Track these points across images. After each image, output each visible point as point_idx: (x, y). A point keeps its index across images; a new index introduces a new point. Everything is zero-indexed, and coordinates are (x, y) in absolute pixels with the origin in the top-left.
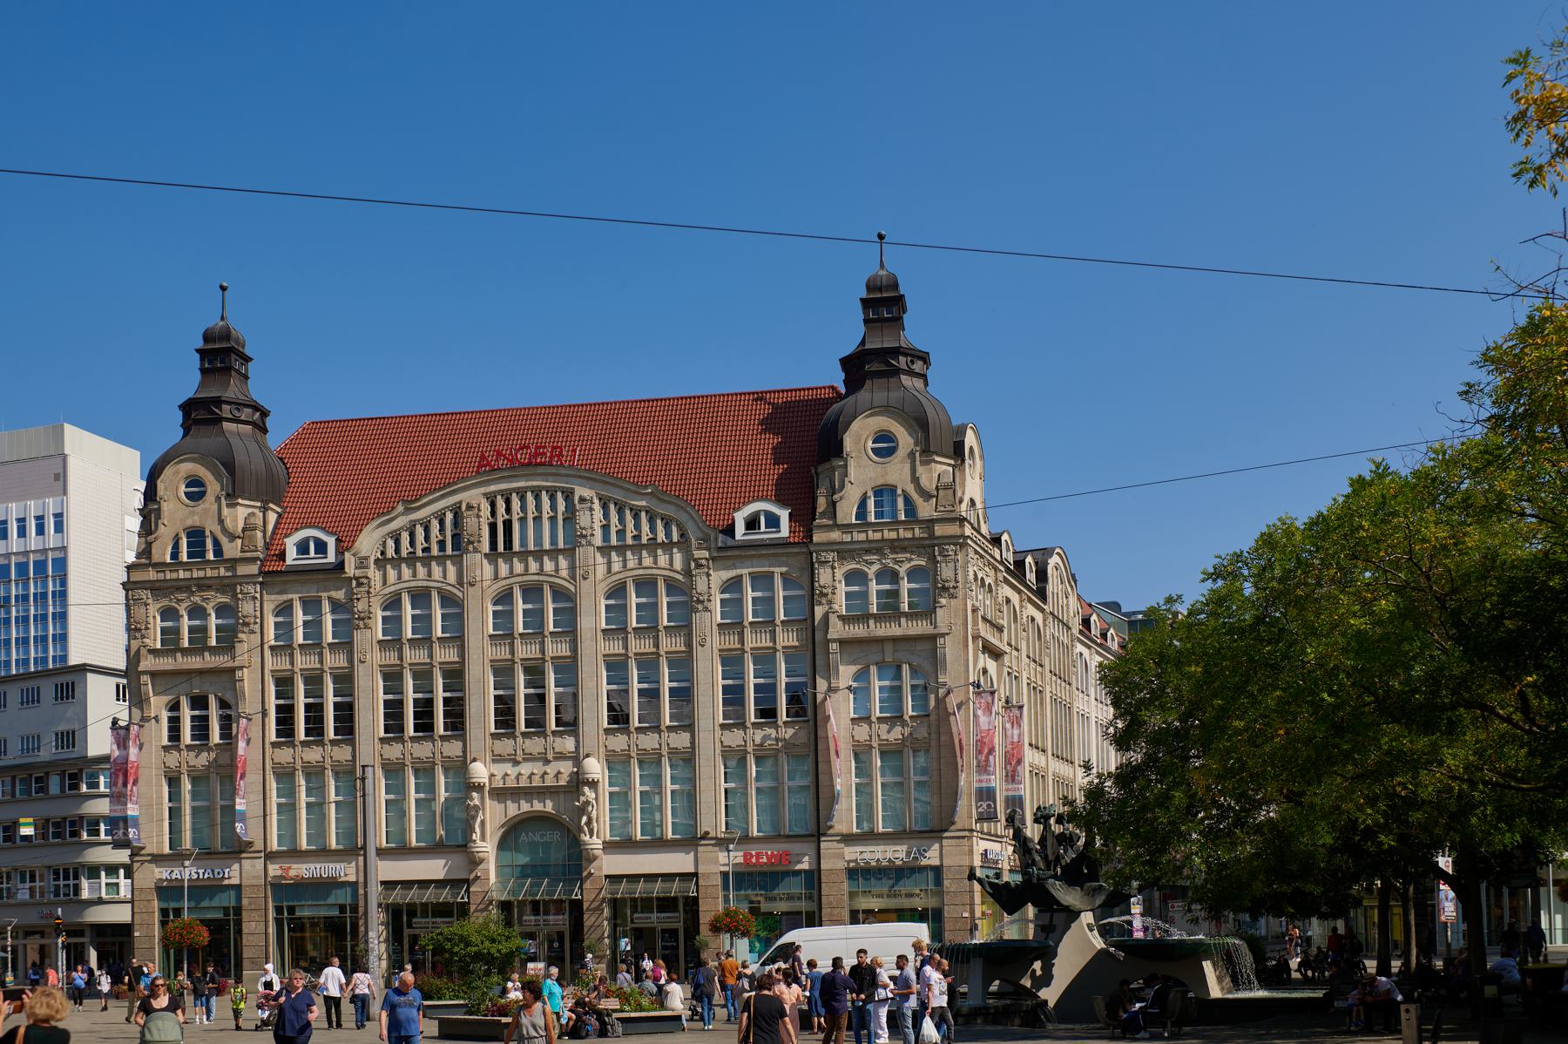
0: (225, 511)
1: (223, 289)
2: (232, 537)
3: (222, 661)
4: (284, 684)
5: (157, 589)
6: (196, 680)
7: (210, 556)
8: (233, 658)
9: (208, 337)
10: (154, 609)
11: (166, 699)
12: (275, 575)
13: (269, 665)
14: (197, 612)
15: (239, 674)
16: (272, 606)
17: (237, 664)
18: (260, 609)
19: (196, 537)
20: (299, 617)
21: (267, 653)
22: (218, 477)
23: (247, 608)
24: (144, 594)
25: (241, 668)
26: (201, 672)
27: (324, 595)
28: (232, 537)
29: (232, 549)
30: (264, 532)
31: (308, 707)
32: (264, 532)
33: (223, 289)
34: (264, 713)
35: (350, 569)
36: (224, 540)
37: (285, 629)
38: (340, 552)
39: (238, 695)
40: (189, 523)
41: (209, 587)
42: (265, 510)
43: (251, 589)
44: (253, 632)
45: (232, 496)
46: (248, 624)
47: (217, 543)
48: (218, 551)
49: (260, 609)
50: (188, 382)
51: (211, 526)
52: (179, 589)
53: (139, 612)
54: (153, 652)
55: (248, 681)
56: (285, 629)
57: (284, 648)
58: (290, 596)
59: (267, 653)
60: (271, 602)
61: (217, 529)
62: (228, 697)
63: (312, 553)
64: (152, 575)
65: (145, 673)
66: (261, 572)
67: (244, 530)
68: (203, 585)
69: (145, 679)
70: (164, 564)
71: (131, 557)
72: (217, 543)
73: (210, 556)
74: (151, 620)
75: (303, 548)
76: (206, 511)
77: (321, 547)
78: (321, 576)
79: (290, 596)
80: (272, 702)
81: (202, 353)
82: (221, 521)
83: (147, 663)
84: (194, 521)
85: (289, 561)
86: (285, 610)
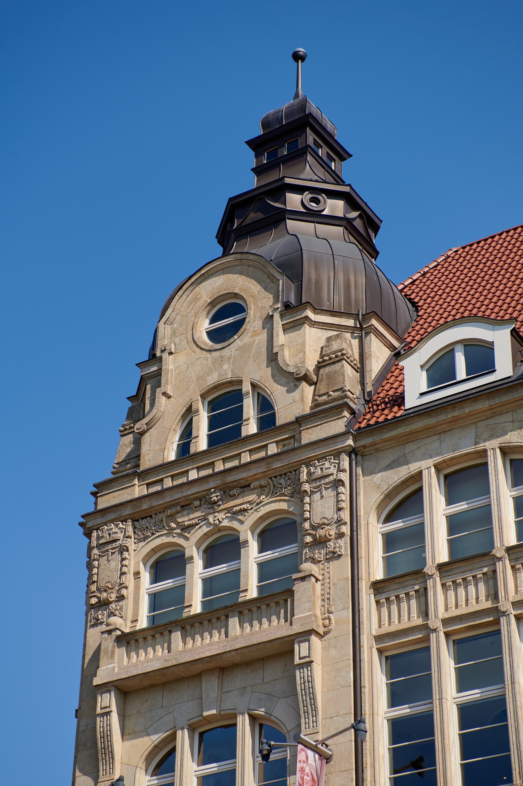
0: (281, 338)
2: (295, 379)
3: (269, 629)
4: (409, 671)
5: (142, 516)
6: (210, 686)
7: (251, 428)
8: (289, 618)
10: (137, 555)
11: (146, 743)
12: (381, 426)
13: (372, 622)
14: (223, 548)
15: (301, 650)
16: (377, 497)
17: (296, 629)
18: (353, 505)
19: (225, 403)
20: (438, 509)
21: (367, 599)
22: (268, 283)
23: (321, 507)
24: (121, 531)
25: (305, 635)
26: (222, 667)
27: (492, 445)
28: (295, 379)
29: (291, 404)
31: (467, 714)
32: (361, 370)
33: (297, 57)
34: (358, 727)
36: (278, 394)
37: (406, 543)
39: (296, 698)
40: (212, 379)
41: (245, 487)
42: (362, 331)
43: (329, 467)
44: (335, 556)
45: (293, 311)
46: (320, 542)
47: (265, 405)
48: (267, 420)
49: (353, 505)
51: (255, 371)
52: (186, 506)
53: (107, 569)
54: (128, 640)
55: (324, 667)
56: (406, 543)
57: (405, 577)
58: (414, 467)
59: (367, 599)
60: (373, 488)
61: (262, 374)
62: (280, 713)
63: (461, 373)
65: (104, 688)
67: (319, 367)
68: (233, 487)
69: (108, 701)
72: (265, 405)
73: (251, 428)
74: (129, 580)
75: (440, 370)
76: (245, 349)
77: (481, 357)
78: (483, 405)
79: (414, 467)
80: (381, 712)
82: (273, 358)
83: (118, 665)
84: (227, 372)
85: (412, 401)
86: (407, 501)
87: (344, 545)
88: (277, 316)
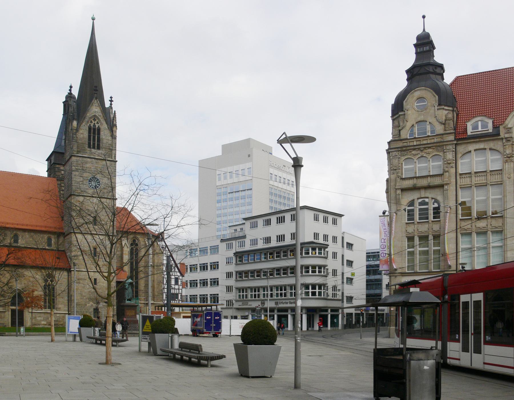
1: (424, 17)
9: (419, 38)
17: (445, 183)
30: (453, 121)
35: (502, 135)
38: (496, 127)
40: (419, 119)
43: (451, 147)
44: (452, 167)
50: (410, 59)
64: (400, 144)
66: (455, 139)
67: (446, 120)
70: (407, 139)
71: (390, 138)
75: (475, 127)
81: (415, 45)
87: (454, 165)
88: (436, 107)
